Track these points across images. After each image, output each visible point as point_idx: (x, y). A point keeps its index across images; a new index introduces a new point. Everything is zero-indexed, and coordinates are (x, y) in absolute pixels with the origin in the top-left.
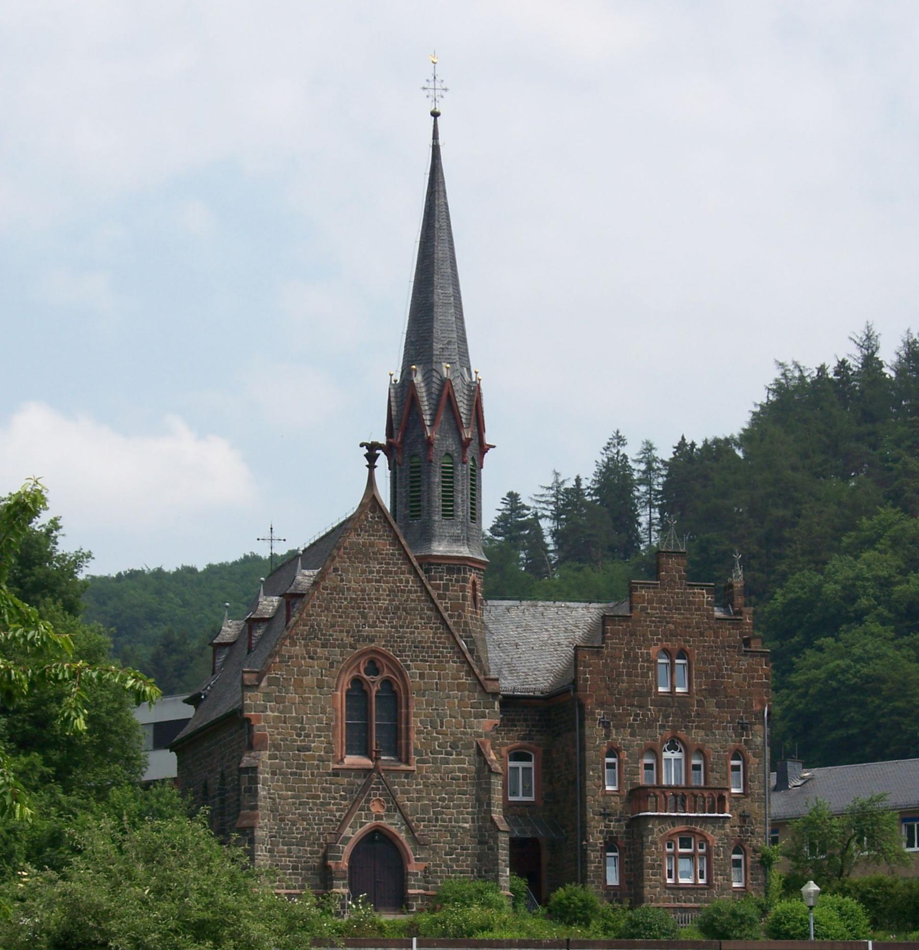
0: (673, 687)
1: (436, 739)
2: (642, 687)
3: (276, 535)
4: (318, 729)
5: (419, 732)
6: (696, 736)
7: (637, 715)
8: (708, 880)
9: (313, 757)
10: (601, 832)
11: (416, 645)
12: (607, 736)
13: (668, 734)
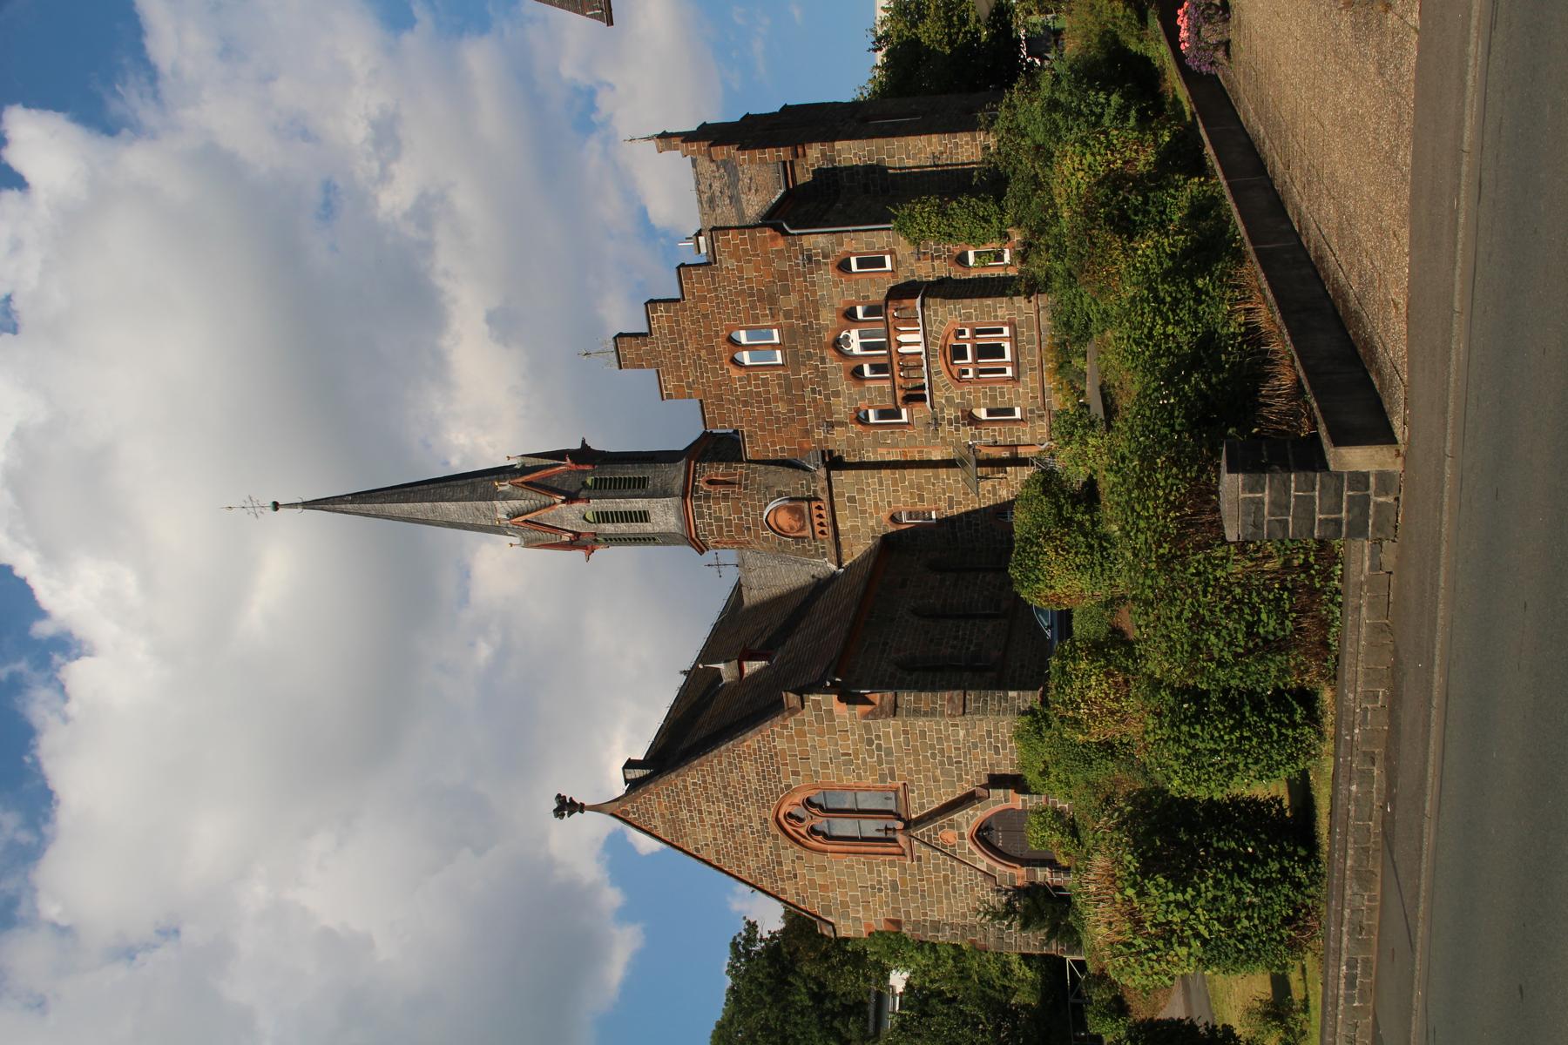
0: (774, 346)
1: (864, 760)
2: (780, 386)
3: (714, 562)
4: (871, 872)
5: (859, 777)
6: (828, 318)
7: (814, 391)
8: (1004, 324)
9: (904, 883)
10: (957, 429)
11: (762, 777)
12: (841, 424)
13: (830, 354)
